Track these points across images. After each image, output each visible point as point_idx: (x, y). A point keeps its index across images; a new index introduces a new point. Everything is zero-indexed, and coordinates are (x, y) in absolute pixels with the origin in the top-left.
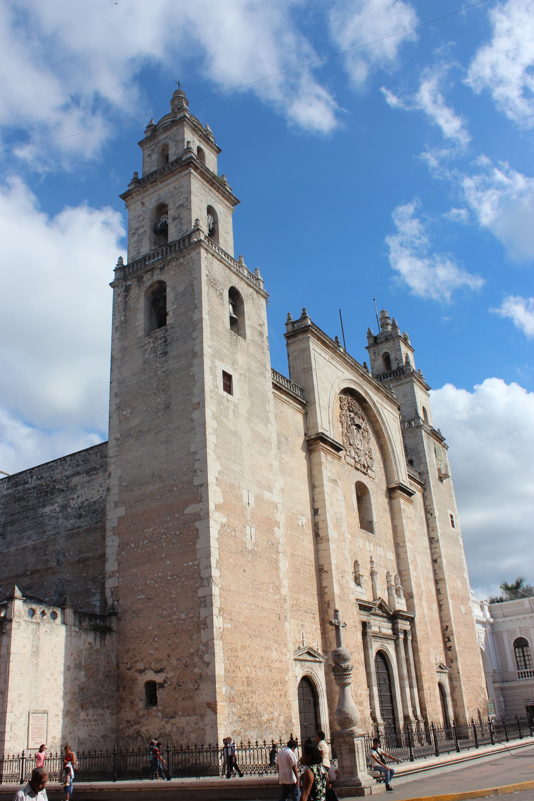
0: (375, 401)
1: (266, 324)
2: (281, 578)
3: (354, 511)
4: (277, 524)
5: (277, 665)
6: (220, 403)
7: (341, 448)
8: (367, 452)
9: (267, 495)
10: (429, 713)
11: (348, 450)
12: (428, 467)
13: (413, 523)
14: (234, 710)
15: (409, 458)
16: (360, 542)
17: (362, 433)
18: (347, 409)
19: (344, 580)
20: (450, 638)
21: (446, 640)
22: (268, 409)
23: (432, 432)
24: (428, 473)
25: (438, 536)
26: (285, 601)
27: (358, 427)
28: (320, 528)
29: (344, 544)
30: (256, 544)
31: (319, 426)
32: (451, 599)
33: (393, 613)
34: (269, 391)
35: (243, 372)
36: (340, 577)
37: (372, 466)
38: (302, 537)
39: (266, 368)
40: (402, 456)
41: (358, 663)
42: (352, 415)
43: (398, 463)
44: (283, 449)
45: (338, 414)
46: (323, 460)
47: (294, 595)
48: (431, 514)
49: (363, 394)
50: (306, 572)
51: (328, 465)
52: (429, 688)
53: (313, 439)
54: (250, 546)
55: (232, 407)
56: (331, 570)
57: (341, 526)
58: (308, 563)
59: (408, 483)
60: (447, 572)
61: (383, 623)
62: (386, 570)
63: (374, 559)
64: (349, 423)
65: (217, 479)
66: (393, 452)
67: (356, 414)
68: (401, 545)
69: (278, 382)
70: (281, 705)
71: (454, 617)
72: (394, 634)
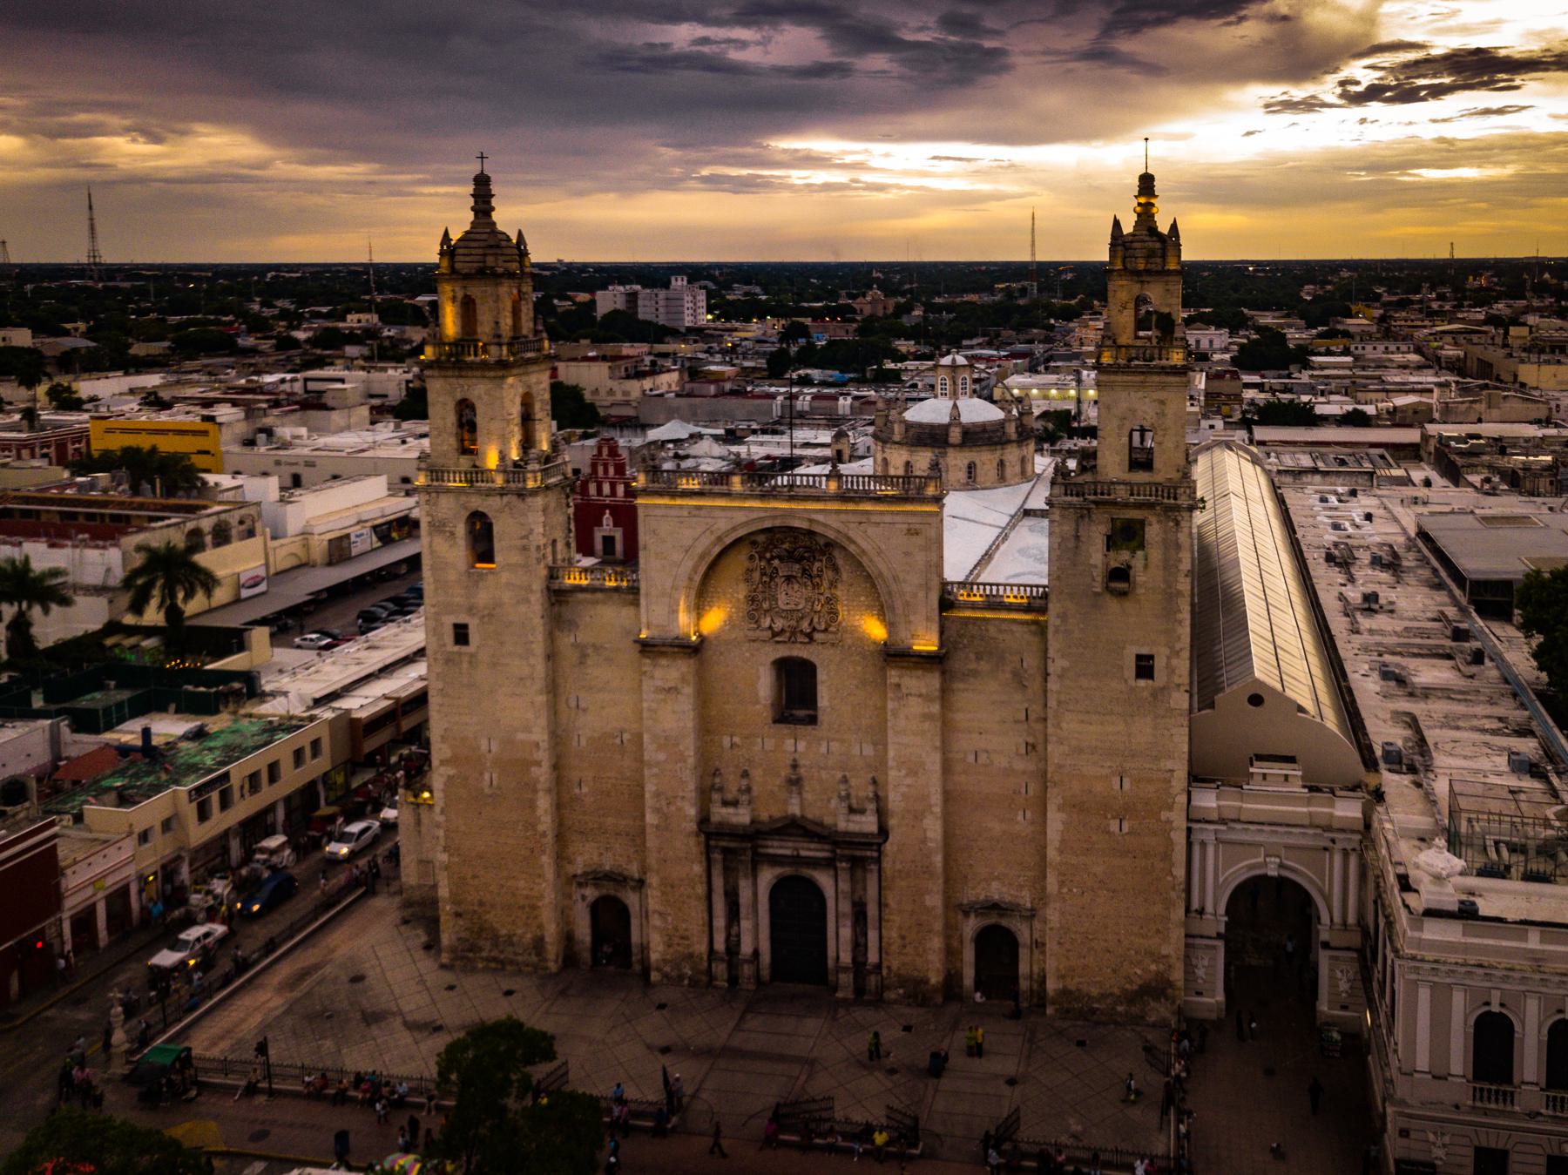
3: (757, 702)
4: (538, 764)
5: (525, 892)
6: (448, 661)
9: (521, 736)
10: (889, 968)
14: (461, 922)
16: (770, 744)
19: (673, 808)
30: (499, 788)
35: (486, 612)
36: (664, 803)
51: (658, 673)
52: (903, 938)
54: (487, 791)
55: (466, 659)
63: (802, 762)
65: (442, 737)
70: (526, 925)
71: (1063, 841)
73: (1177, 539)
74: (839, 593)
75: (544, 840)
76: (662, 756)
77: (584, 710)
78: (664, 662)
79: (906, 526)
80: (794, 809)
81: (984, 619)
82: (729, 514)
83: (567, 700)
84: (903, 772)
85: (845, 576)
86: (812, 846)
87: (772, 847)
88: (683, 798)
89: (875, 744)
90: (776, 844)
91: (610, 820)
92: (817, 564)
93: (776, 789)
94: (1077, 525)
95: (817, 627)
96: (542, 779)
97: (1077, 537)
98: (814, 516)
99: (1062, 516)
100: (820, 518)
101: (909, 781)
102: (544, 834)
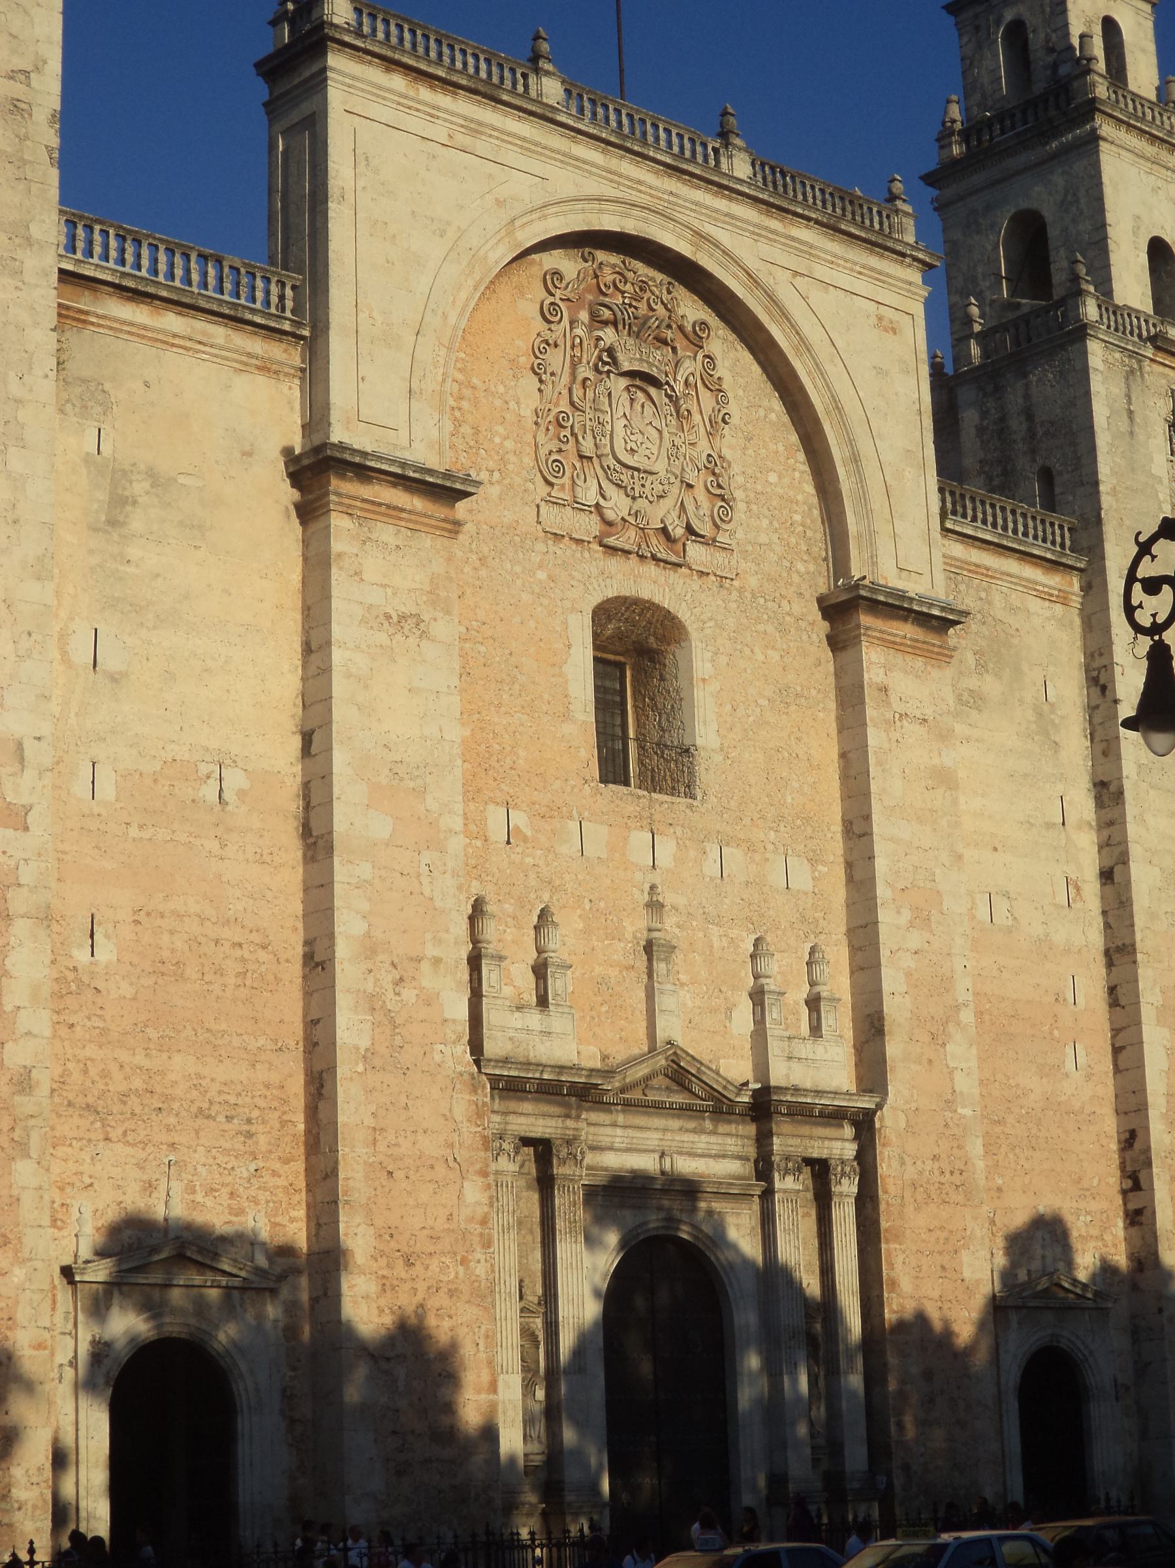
0: (752, 264)
1: (55, 65)
2: (8, 1008)
3: (566, 716)
7: (458, 486)
8: (691, 477)
10: (906, 1468)
11: (566, 480)
12: (1106, 501)
13: (944, 736)
15: (1040, 461)
16: (598, 836)
17: (674, 400)
18: (584, 316)
19: (408, 994)
20: (1142, 1176)
21: (1129, 1184)
22: (15, 389)
23: (1158, 348)
24: (1099, 521)
25: (1120, 779)
26: (24, 1083)
27: (643, 379)
28: (312, 804)
29: (426, 857)
31: (335, 416)
32: (1160, 1022)
33: (753, 1096)
34: (36, 324)
36: (387, 978)
37: (717, 527)
38: (214, 845)
39: (29, 241)
40: (910, 474)
41: (452, 1293)
42: (609, 335)
43: (877, 501)
44: (137, 523)
45: (523, 345)
46: (336, 546)
47: (140, 1059)
48: (1104, 688)
49: (684, 248)
50: (219, 972)
51: (373, 565)
53: (309, 468)
56: (332, 959)
57: (421, 792)
58: (237, 939)
59: (940, 577)
60: (1153, 916)
61: (686, 1137)
62: (754, 932)
63: (667, 897)
64: (584, 372)
66: (855, 459)
67: (637, 329)
68: (857, 829)
69: (124, 275)
72: (760, 1176)
74: (726, 452)
75: (25, 1104)
76: (380, 827)
77: (115, 679)
78: (386, 533)
80: (669, 1028)
81: (986, 573)
82: (535, 166)
83: (63, 637)
84: (906, 915)
86: (702, 1142)
87: (611, 1149)
88: (437, 961)
89: (813, 862)
90: (619, 1136)
91: (181, 1065)
93: (613, 973)
94: (1128, 387)
95: (696, 525)
96: (27, 875)
97: (1130, 413)
98: (709, 229)
100: (723, 236)
101: (915, 940)
102: (24, 1083)
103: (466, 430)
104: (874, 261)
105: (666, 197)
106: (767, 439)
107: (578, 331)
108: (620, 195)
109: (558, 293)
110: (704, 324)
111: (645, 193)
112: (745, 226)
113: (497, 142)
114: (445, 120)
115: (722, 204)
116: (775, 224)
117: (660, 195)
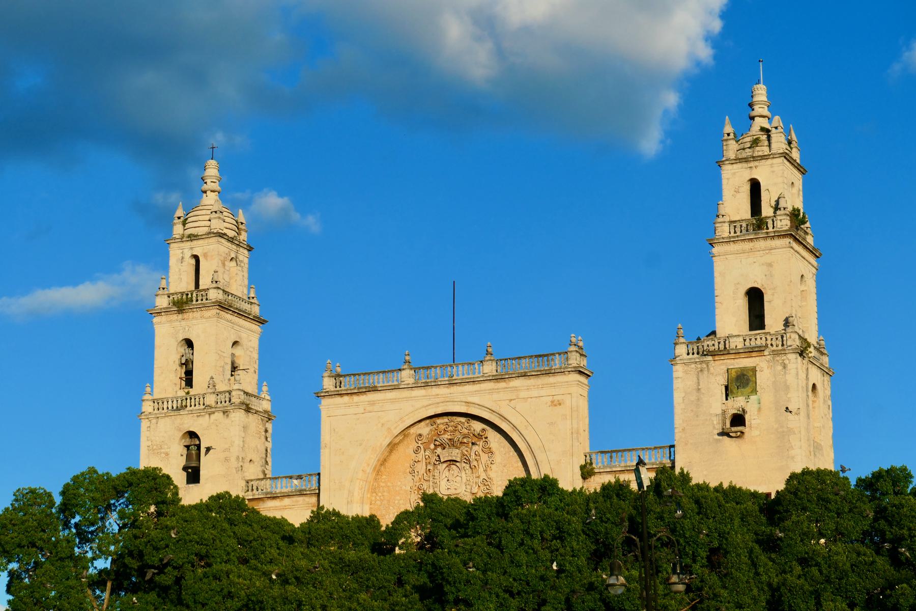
73: (785, 382)
74: (492, 474)
79: (550, 398)
85: (498, 458)
92: (475, 448)
99: (686, 372)
100: (475, 399)
103: (385, 502)
104: (551, 379)
105: (449, 395)
106: (513, 463)
107: (427, 453)
108: (430, 402)
109: (420, 442)
110: (484, 430)
111: (441, 397)
112: (485, 392)
113: (382, 404)
114: (362, 405)
115: (476, 387)
116: (502, 385)
117: (447, 396)
